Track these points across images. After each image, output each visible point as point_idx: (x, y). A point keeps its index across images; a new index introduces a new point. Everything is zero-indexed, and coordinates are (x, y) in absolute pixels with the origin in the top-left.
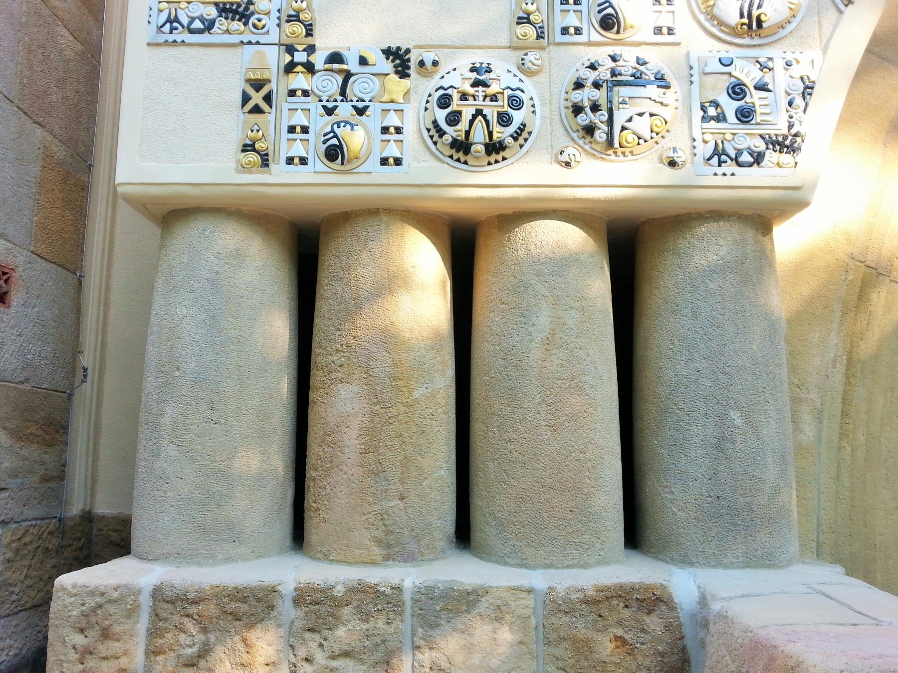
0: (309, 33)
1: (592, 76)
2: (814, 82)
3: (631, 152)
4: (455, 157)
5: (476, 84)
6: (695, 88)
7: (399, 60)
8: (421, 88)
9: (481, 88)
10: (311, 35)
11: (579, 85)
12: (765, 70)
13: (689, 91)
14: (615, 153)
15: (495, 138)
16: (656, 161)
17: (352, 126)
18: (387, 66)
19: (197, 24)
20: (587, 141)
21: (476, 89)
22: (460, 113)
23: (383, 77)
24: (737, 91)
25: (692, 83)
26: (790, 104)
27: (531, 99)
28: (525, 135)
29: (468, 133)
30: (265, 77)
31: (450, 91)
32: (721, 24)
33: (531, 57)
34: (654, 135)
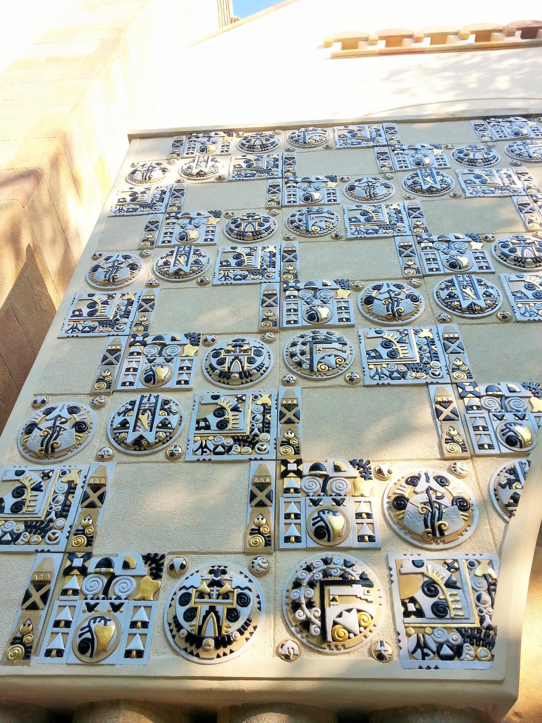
0: (90, 543)
1: (307, 577)
2: (496, 580)
3: (343, 646)
4: (189, 651)
5: (212, 584)
6: (395, 586)
7: (155, 563)
8: (169, 586)
9: (215, 588)
10: (91, 545)
11: (297, 584)
12: (452, 570)
13: (390, 589)
14: (329, 646)
15: (223, 633)
16: (366, 654)
17: (106, 621)
18: (143, 569)
19: (8, 537)
20: (304, 635)
21: (211, 588)
22: (195, 609)
23: (139, 578)
24: (430, 588)
25: (392, 582)
26: (479, 598)
27: (258, 597)
28: (250, 629)
29: (200, 628)
30: (46, 579)
31: (190, 591)
32: (410, 532)
33: (259, 561)
34: (362, 629)
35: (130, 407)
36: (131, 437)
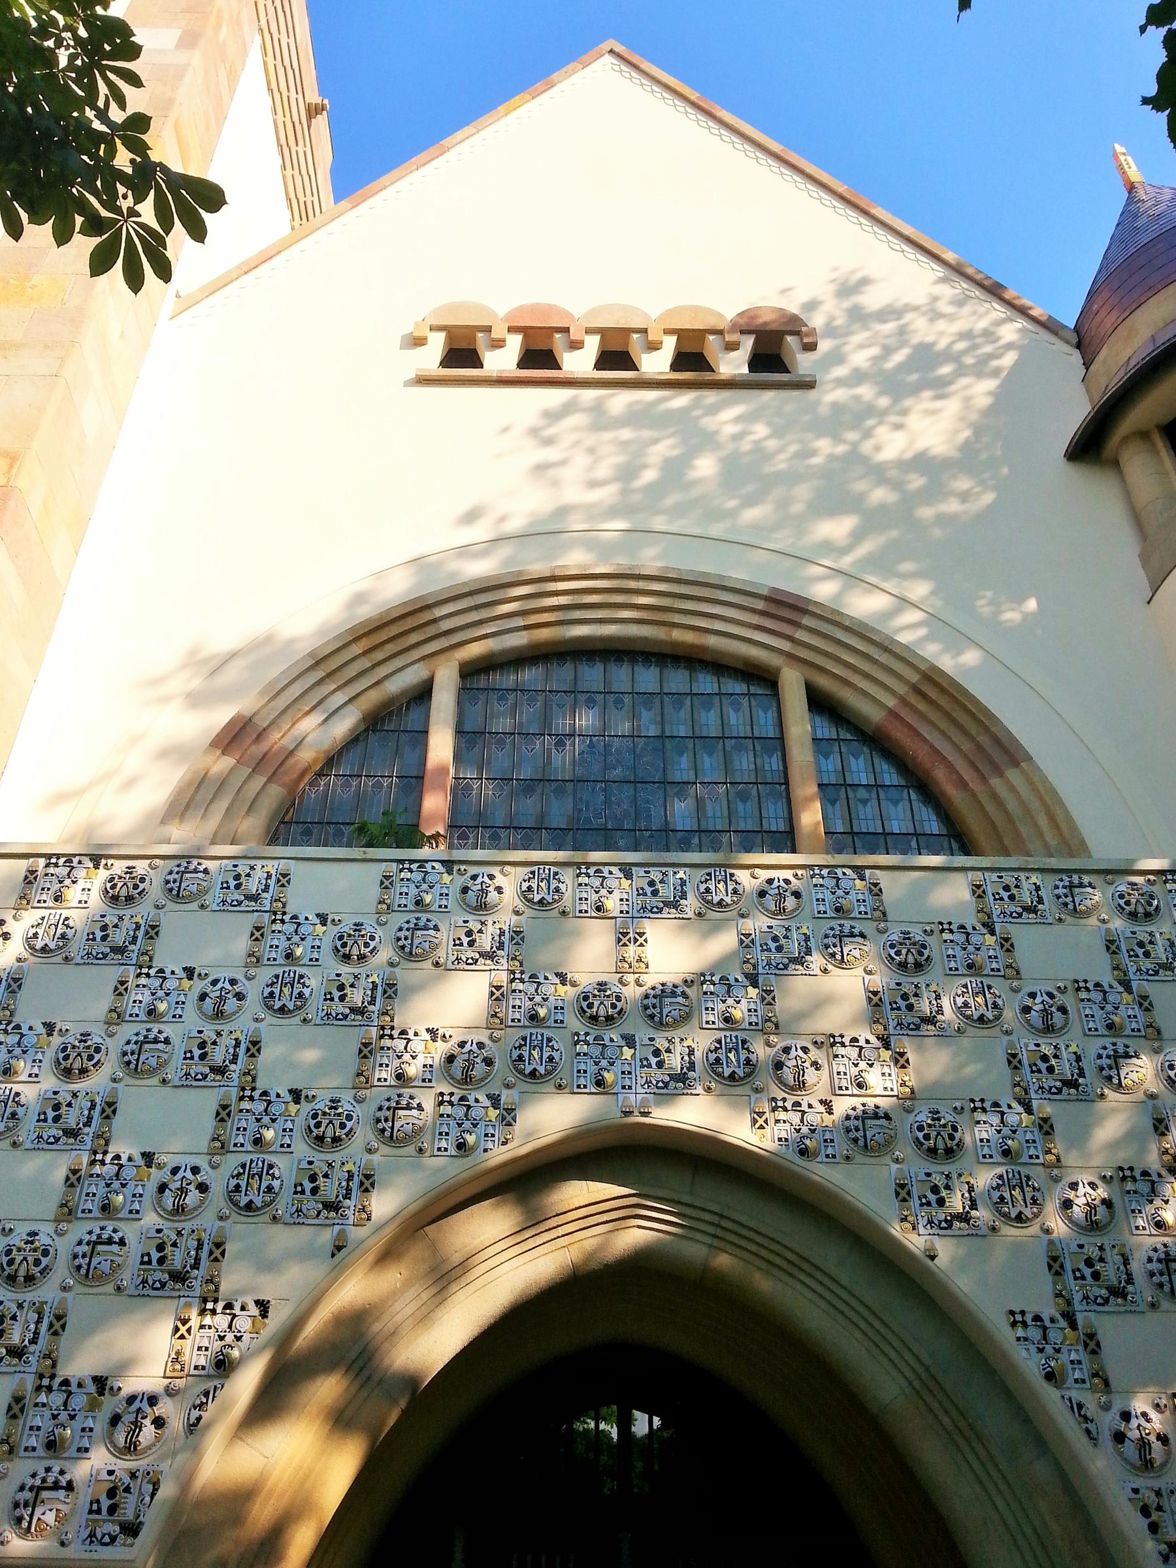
36: (244, 1201)
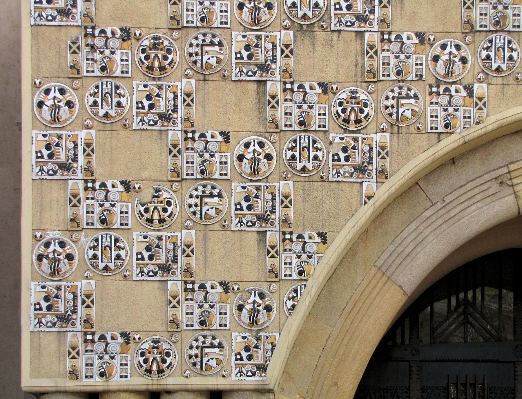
28: (173, 215)
29: (152, 216)
35: (96, 91)
